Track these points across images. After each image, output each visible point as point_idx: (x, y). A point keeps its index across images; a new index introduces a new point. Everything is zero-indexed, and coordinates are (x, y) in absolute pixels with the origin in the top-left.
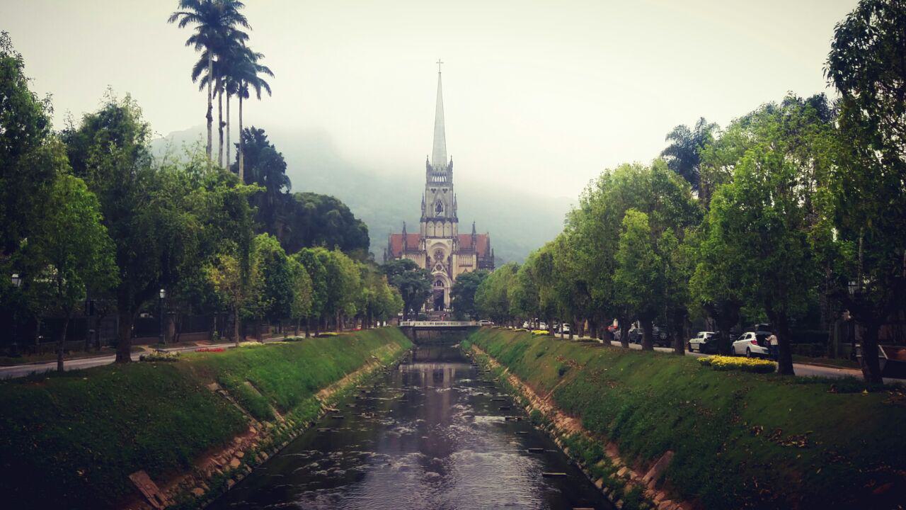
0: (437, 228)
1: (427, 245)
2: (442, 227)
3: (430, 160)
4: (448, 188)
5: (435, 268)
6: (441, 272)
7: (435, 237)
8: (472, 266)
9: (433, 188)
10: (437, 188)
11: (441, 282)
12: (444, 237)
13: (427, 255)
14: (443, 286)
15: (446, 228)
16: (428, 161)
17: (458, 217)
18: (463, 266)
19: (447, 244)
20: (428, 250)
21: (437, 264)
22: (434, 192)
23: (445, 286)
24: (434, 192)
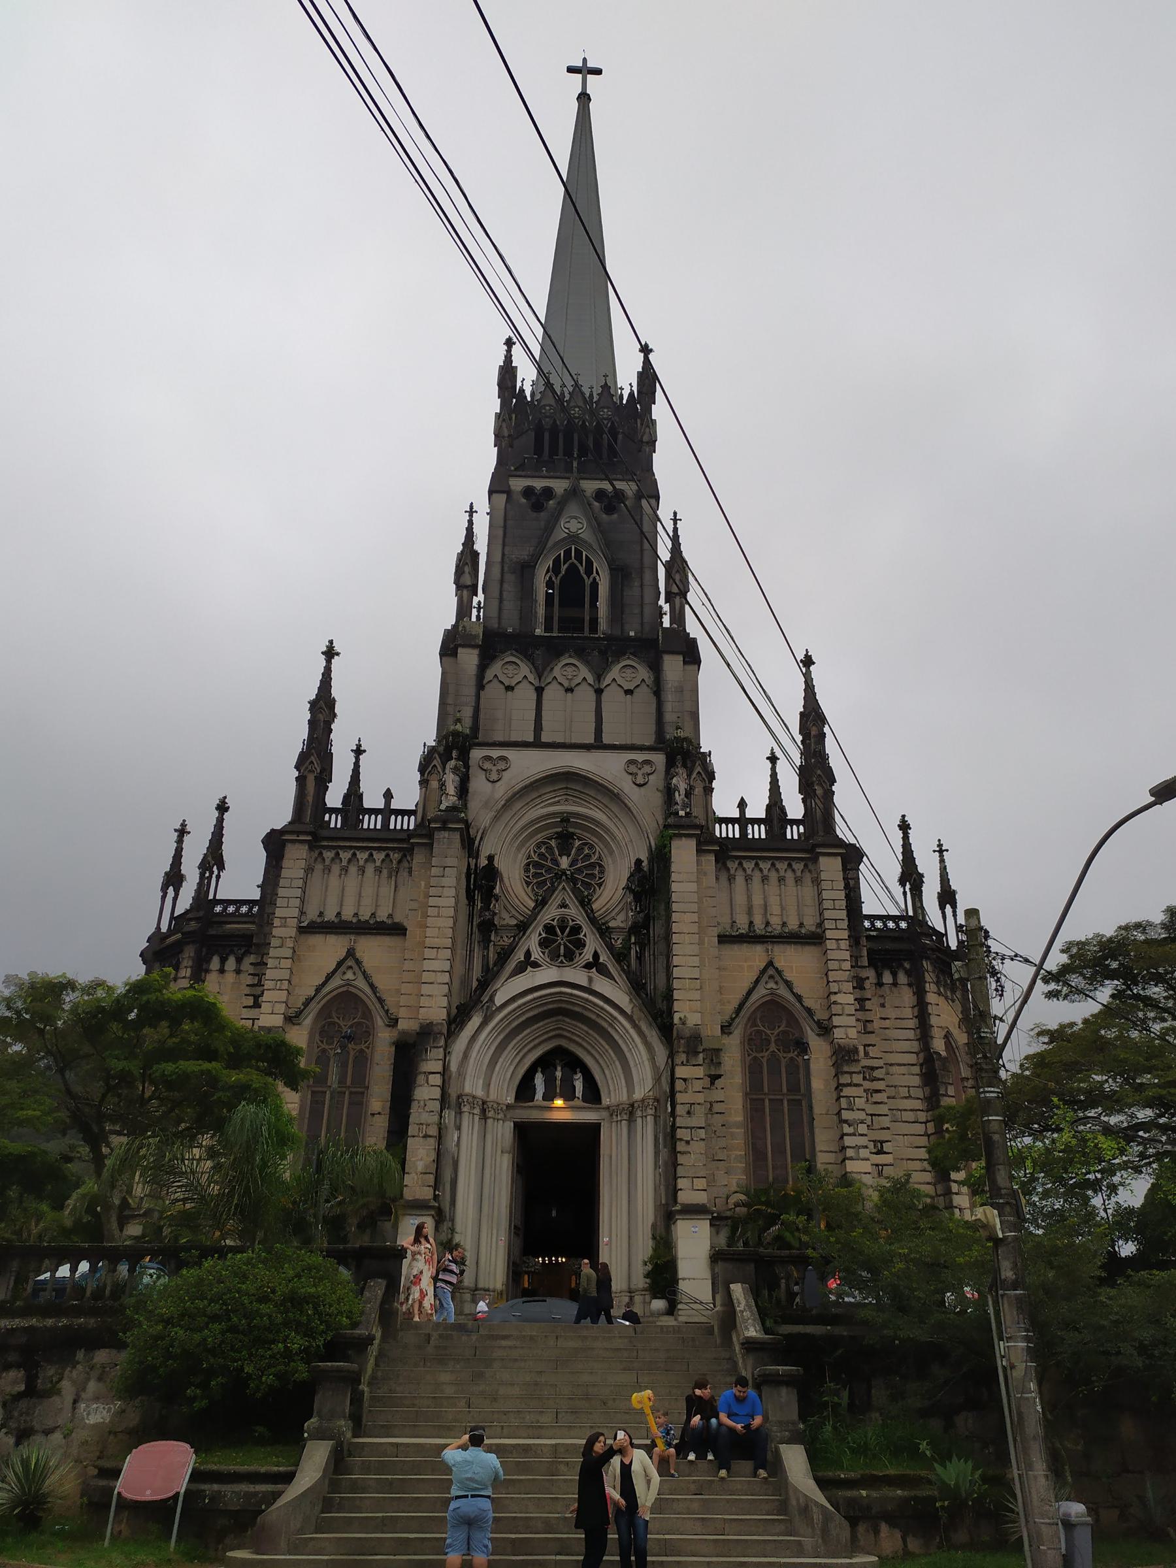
0: (552, 694)
1: (479, 784)
2: (586, 695)
3: (527, 375)
4: (628, 488)
5: (532, 942)
6: (577, 975)
7: (537, 744)
8: (815, 939)
9: (538, 484)
10: (560, 486)
11: (575, 1064)
12: (598, 745)
13: (470, 845)
14: (593, 1095)
15: (613, 700)
16: (507, 373)
17: (692, 628)
18: (750, 938)
19: (625, 785)
20: (479, 814)
21: (551, 914)
22: (538, 507)
23: (614, 1093)
24: (538, 507)
